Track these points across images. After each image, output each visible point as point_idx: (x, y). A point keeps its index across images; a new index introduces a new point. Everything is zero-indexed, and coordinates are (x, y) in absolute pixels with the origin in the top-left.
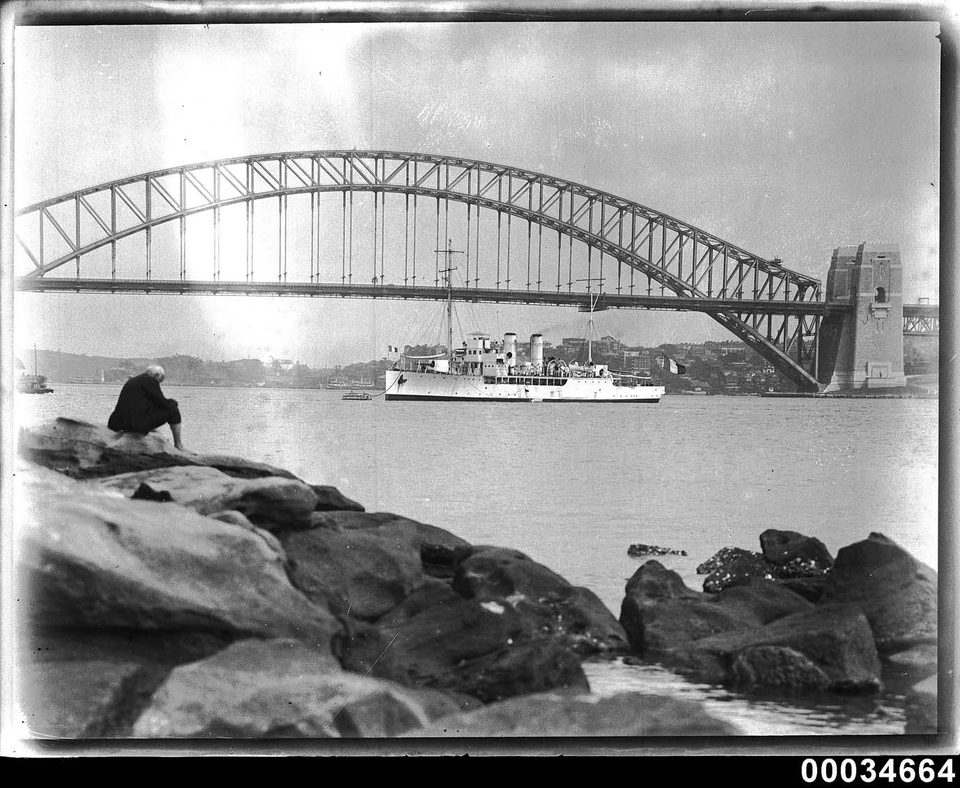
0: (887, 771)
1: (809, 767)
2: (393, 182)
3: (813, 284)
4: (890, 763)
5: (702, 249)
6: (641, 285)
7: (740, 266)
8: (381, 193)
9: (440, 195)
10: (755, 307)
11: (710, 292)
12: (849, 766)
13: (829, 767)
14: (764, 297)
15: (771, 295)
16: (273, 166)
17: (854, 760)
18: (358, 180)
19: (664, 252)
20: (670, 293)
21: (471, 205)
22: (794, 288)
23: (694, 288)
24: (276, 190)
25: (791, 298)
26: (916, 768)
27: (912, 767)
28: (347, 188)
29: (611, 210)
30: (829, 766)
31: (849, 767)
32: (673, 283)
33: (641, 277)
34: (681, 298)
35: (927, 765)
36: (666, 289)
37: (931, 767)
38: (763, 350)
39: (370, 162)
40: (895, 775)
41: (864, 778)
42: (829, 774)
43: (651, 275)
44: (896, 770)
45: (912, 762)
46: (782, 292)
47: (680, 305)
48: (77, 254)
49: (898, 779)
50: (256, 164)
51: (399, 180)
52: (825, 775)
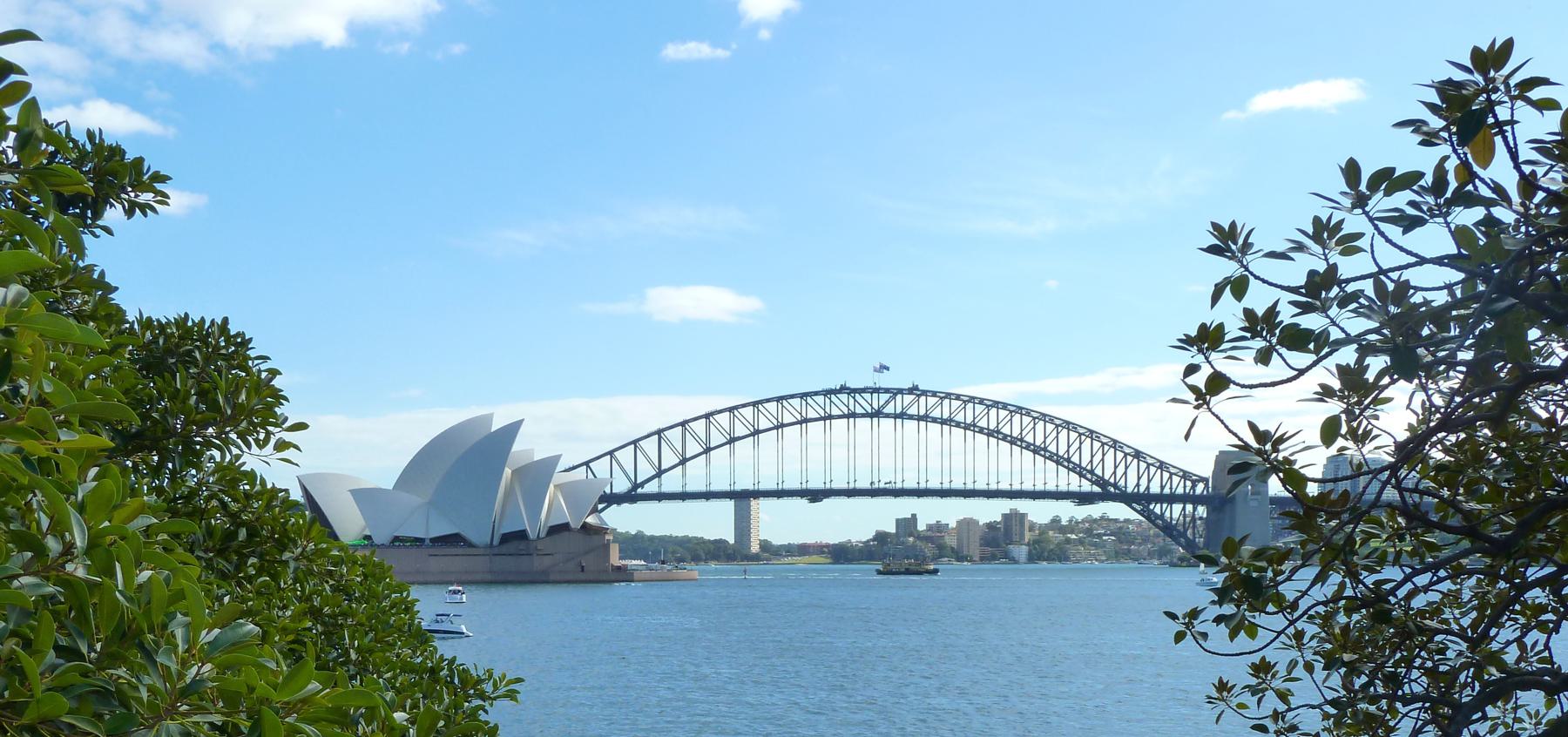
2: (885, 411)
5: (1120, 455)
7: (1148, 467)
9: (919, 418)
10: (1160, 498)
14: (1167, 491)
18: (859, 410)
20: (1096, 489)
22: (1189, 484)
23: (1115, 485)
25: (1187, 491)
28: (853, 415)
32: (1101, 482)
33: (1074, 477)
36: (1094, 486)
38: (1168, 529)
39: (867, 396)
43: (1081, 475)
47: (1105, 497)
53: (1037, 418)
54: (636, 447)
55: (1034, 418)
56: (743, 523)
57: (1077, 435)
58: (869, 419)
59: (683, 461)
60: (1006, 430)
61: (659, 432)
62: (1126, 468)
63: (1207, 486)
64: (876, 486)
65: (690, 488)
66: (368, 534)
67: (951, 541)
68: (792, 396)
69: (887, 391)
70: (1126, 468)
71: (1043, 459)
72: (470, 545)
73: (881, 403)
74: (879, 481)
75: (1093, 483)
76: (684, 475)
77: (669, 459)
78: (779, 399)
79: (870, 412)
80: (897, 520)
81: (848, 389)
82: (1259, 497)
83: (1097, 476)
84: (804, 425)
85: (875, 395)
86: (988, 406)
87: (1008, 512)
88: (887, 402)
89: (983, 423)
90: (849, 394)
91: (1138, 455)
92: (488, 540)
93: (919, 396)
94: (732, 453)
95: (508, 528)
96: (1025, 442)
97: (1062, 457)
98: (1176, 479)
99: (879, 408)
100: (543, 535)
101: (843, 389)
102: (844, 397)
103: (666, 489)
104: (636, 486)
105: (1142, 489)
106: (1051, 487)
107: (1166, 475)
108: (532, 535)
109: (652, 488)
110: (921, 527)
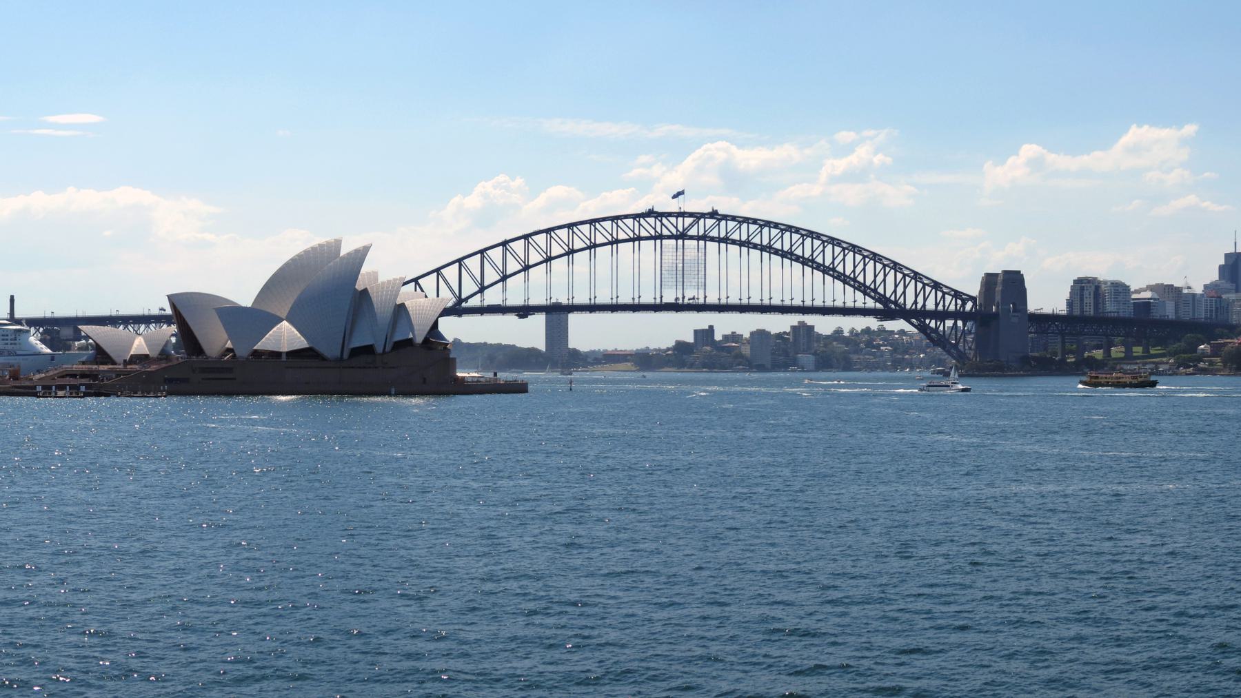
2: (690, 233)
3: (973, 299)
5: (899, 276)
7: (924, 288)
9: (719, 240)
14: (940, 307)
18: (665, 232)
20: (879, 306)
22: (959, 302)
23: (896, 303)
28: (661, 237)
32: (882, 299)
33: (859, 295)
39: (673, 220)
43: (865, 294)
46: (951, 304)
48: (482, 289)
53: (826, 241)
54: (460, 266)
55: (823, 242)
56: (556, 333)
57: (861, 257)
58: (674, 241)
59: (504, 278)
60: (799, 252)
61: (482, 252)
62: (905, 287)
63: (975, 304)
64: (680, 301)
65: (511, 302)
66: (231, 347)
67: (746, 350)
69: (691, 215)
70: (905, 287)
71: (832, 278)
72: (324, 359)
73: (685, 226)
74: (683, 298)
75: (877, 301)
76: (504, 289)
77: (491, 276)
78: (592, 222)
79: (674, 231)
80: (696, 332)
81: (656, 213)
82: (1019, 314)
83: (879, 294)
84: (615, 246)
85: (680, 219)
86: (782, 230)
87: (796, 324)
88: (691, 225)
89: (778, 246)
90: (656, 218)
91: (916, 276)
92: (338, 354)
93: (719, 220)
95: (358, 341)
96: (816, 263)
97: (849, 277)
98: (948, 298)
99: (684, 230)
100: (388, 348)
101: (651, 213)
102: (651, 220)
103: (486, 303)
104: (460, 300)
105: (919, 306)
106: (839, 304)
107: (940, 294)
108: (379, 349)
109: (475, 302)
110: (718, 337)
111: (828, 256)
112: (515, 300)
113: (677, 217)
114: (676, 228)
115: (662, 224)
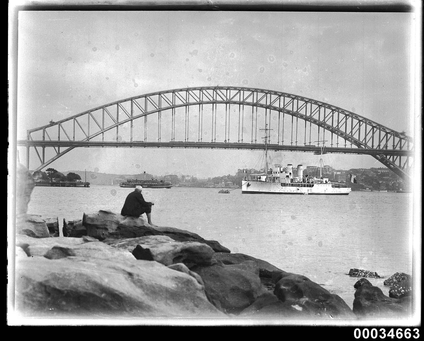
0: (391, 334)
1: (357, 332)
2: (233, 100)
4: (392, 330)
6: (341, 143)
8: (229, 104)
11: (373, 146)
12: (374, 331)
13: (366, 332)
15: (401, 147)
16: (183, 94)
17: (377, 329)
18: (219, 99)
19: (352, 129)
20: (355, 147)
21: (267, 109)
23: (366, 145)
24: (184, 103)
26: (403, 332)
27: (401, 332)
28: (214, 102)
29: (328, 111)
30: (366, 331)
31: (374, 332)
33: (341, 140)
34: (360, 149)
35: (408, 331)
37: (410, 332)
39: (224, 91)
40: (394, 335)
41: (381, 336)
42: (366, 335)
43: (346, 139)
44: (395, 333)
45: (401, 330)
47: (359, 152)
49: (395, 337)
50: (176, 93)
51: (236, 99)
52: (359, 331)
68: (181, 90)
77: (109, 123)
79: (225, 99)
94: (146, 120)
103: (105, 140)
104: (88, 138)
109: (98, 139)
111: (320, 115)
112: (126, 139)
113: (227, 90)
114: (226, 97)
115: (217, 93)
